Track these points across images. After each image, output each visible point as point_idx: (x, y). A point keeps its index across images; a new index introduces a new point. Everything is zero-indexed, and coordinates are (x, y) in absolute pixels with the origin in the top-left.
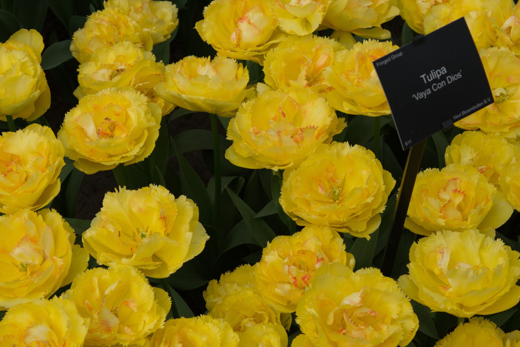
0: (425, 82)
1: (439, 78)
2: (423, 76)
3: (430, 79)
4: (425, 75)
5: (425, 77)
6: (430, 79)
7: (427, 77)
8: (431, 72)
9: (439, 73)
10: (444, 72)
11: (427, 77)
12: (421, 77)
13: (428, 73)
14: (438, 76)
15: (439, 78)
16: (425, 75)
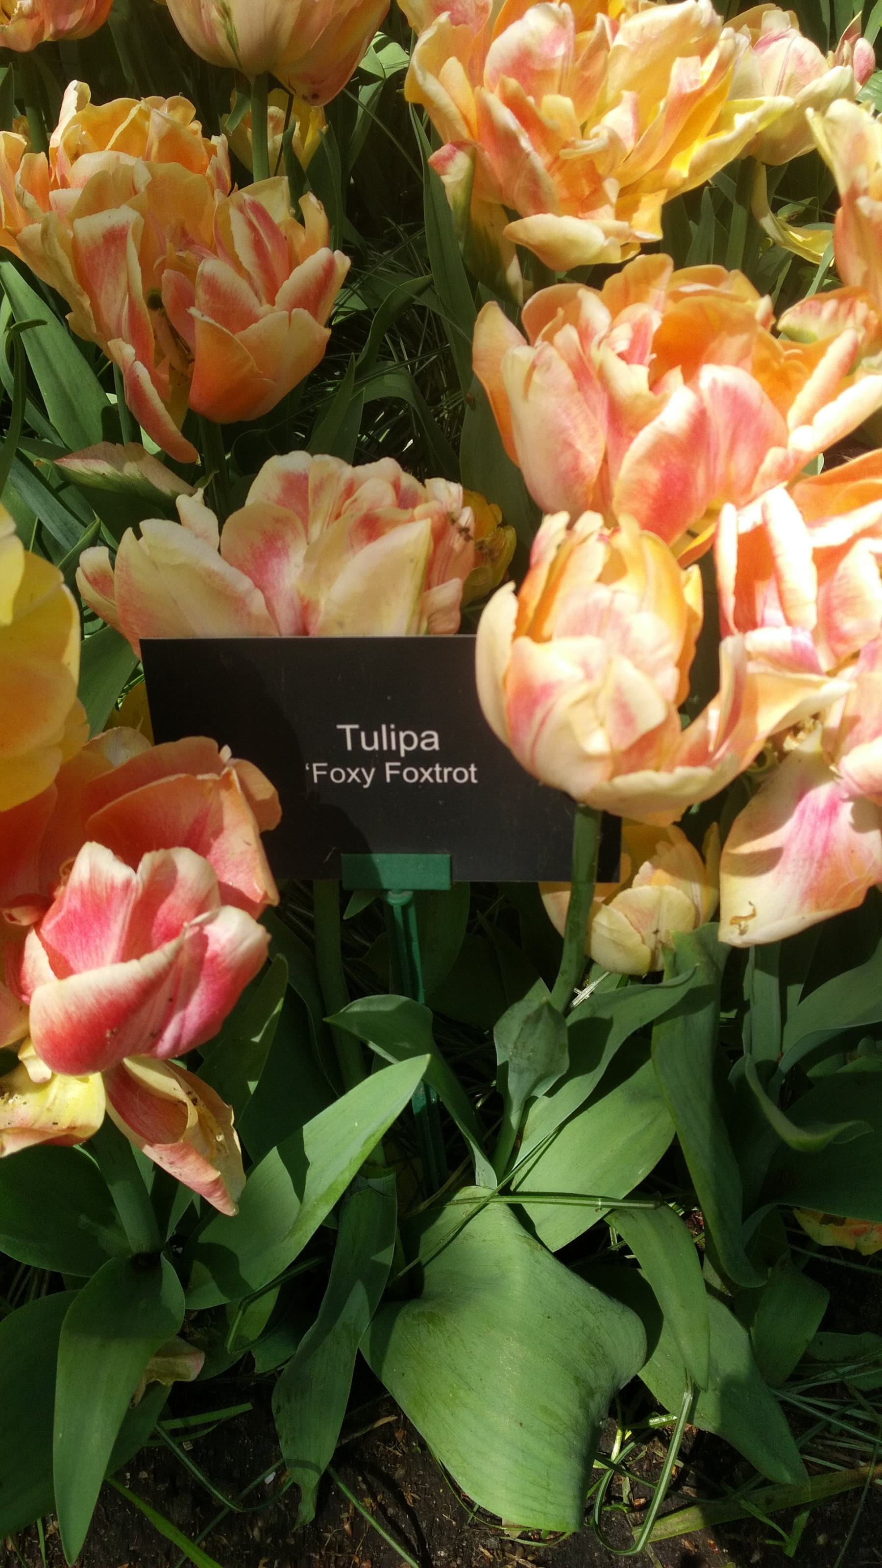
0: (349, 747)
1: (403, 754)
2: (348, 728)
3: (370, 743)
4: (356, 726)
5: (355, 734)
6: (370, 743)
7: (363, 734)
8: (384, 728)
9: (409, 741)
10: (427, 745)
11: (363, 734)
12: (339, 727)
13: (370, 727)
14: (403, 747)
15: (403, 754)
16: (356, 726)
